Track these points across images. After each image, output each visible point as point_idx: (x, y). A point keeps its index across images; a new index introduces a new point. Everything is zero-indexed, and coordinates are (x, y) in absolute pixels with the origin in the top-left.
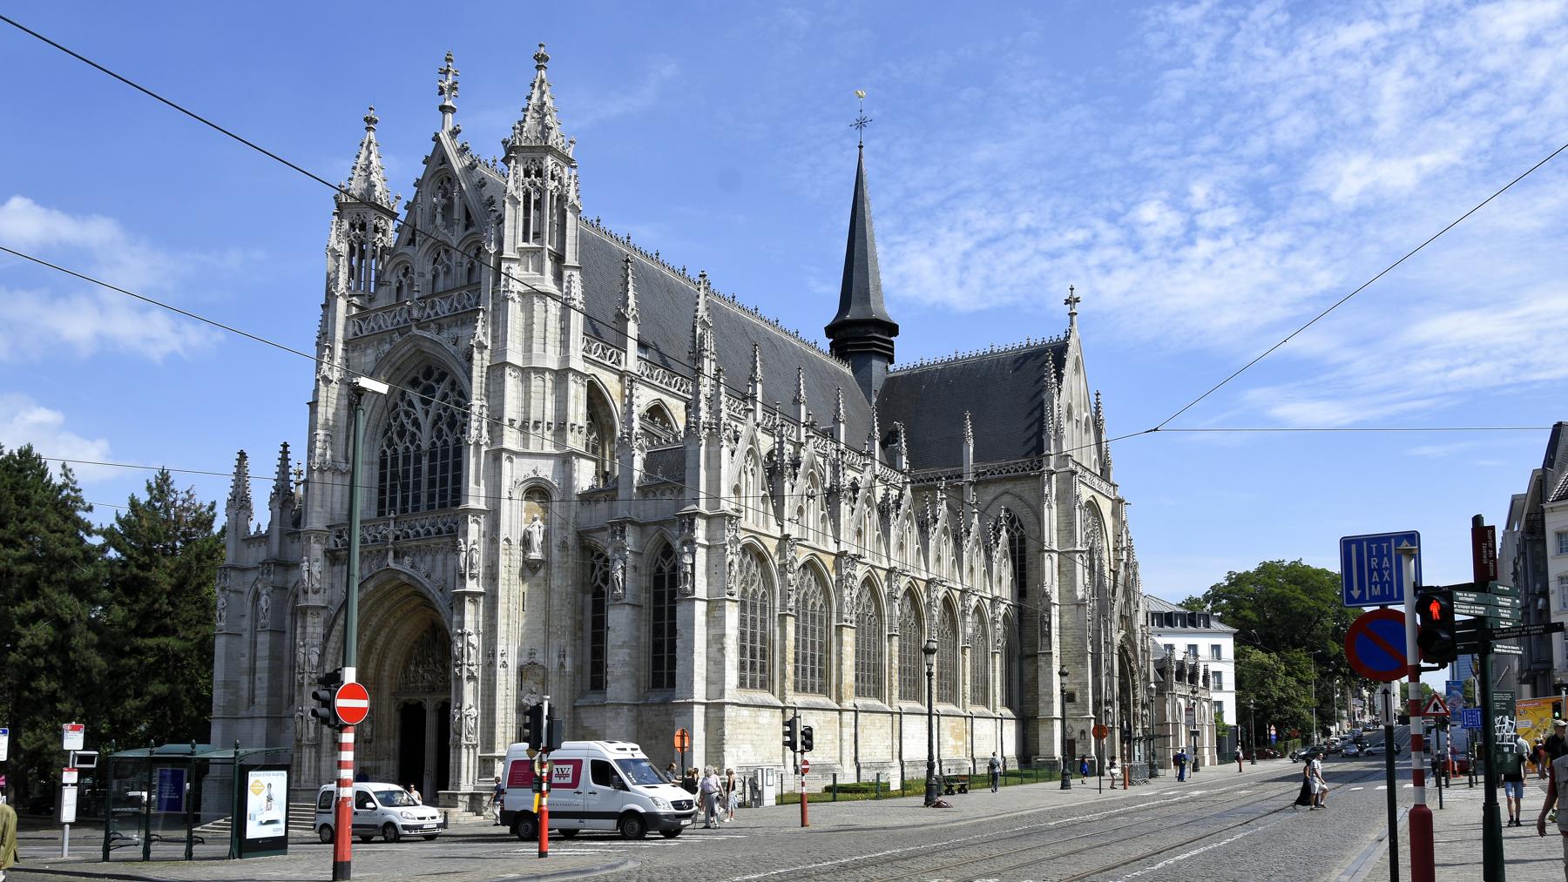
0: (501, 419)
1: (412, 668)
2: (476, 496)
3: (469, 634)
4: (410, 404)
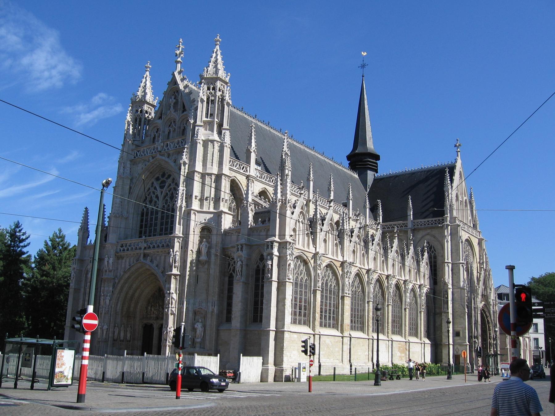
0: (191, 196)
1: (149, 308)
2: (179, 230)
3: (172, 293)
4: (155, 188)
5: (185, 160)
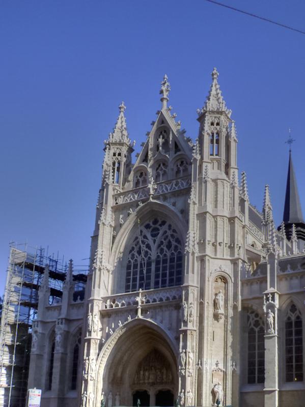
2: (192, 279)
4: (145, 237)
5: (194, 200)
